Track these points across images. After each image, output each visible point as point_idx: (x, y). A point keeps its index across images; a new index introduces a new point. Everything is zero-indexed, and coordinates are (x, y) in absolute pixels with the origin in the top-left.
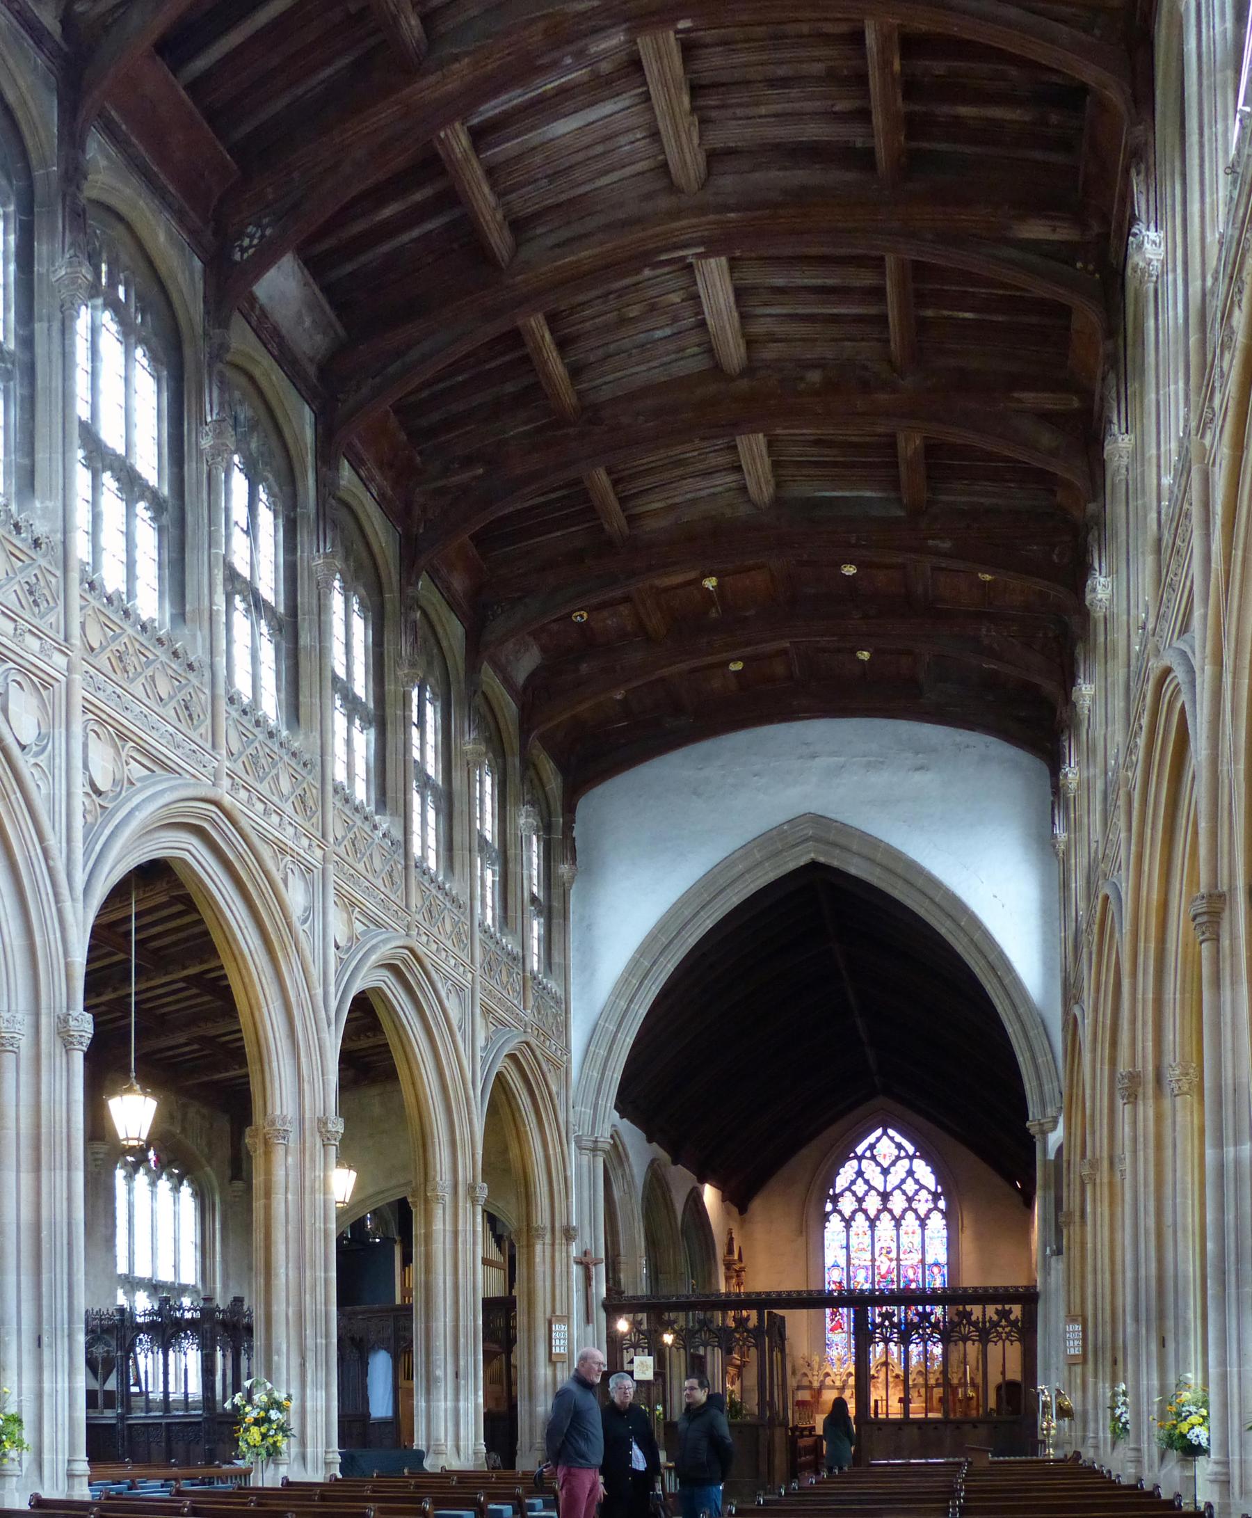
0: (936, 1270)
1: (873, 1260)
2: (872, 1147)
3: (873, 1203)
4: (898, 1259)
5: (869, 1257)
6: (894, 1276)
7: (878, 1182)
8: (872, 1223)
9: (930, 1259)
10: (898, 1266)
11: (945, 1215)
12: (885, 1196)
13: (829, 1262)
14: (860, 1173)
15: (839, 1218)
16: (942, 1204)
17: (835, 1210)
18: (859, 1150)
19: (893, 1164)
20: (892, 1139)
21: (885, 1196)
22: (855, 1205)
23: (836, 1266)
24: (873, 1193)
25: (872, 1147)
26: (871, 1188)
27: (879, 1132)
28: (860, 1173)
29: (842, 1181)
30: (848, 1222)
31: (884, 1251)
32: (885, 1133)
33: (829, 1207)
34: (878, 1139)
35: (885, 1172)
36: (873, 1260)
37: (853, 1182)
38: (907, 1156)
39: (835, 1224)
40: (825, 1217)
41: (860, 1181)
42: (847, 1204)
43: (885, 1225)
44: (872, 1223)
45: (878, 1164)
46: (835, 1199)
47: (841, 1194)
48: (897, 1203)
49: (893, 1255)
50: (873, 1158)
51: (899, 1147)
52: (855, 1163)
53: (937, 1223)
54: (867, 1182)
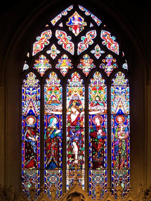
0: (120, 119)
1: (64, 110)
2: (64, 19)
3: (64, 66)
4: (87, 110)
5: (60, 107)
6: (83, 123)
7: (70, 47)
8: (64, 80)
9: (114, 110)
10: (87, 115)
11: (127, 74)
12: (76, 59)
13: (26, 110)
14: (54, 40)
15: (34, 76)
16: (125, 66)
17: (32, 69)
18: (54, 22)
19: (83, 33)
20: (82, 13)
21: (76, 59)
22: (49, 66)
23: (31, 114)
24: (65, 56)
25: (64, 19)
26: (63, 52)
27: (71, 7)
28: (54, 40)
29: (37, 47)
30: (42, 79)
31: (74, 104)
32: (76, 9)
33: (26, 67)
34: (70, 13)
35: (76, 40)
36: (64, 110)
37: (48, 47)
38: (96, 27)
39: (31, 80)
40: (24, 75)
41: (54, 47)
42: (42, 66)
43: (75, 81)
44: (64, 80)
45: (70, 33)
46: (32, 61)
47: (37, 57)
48: (87, 66)
49: (83, 106)
50: (65, 29)
51: (88, 20)
52: (49, 33)
53: (120, 80)
54: (59, 47)
